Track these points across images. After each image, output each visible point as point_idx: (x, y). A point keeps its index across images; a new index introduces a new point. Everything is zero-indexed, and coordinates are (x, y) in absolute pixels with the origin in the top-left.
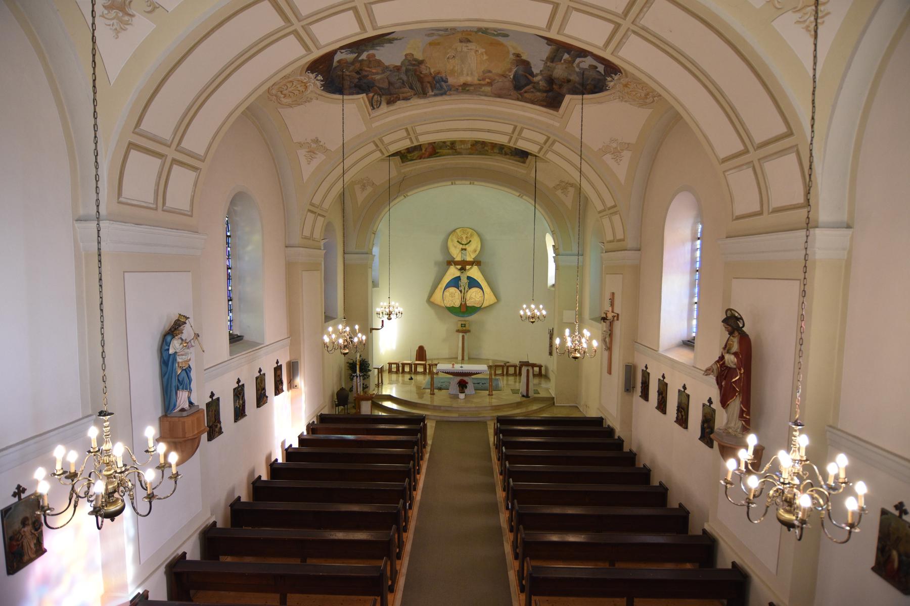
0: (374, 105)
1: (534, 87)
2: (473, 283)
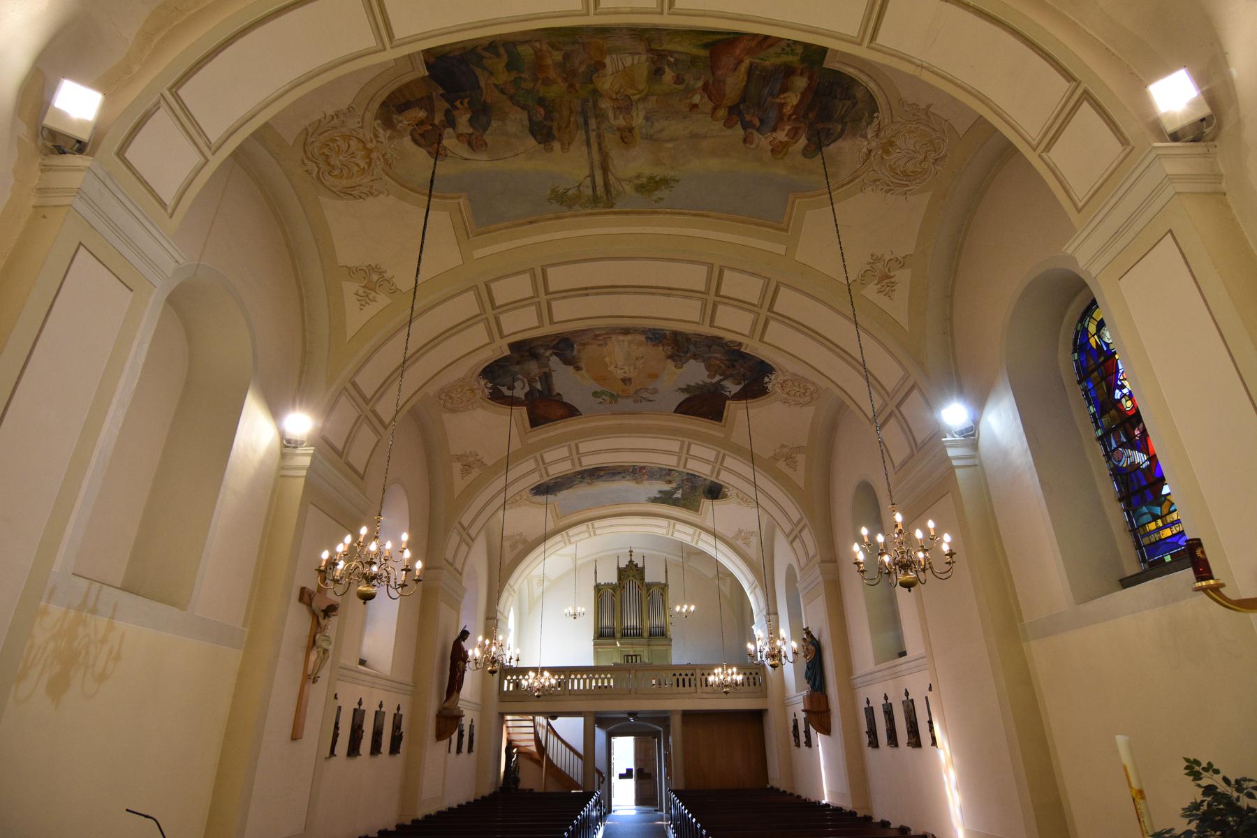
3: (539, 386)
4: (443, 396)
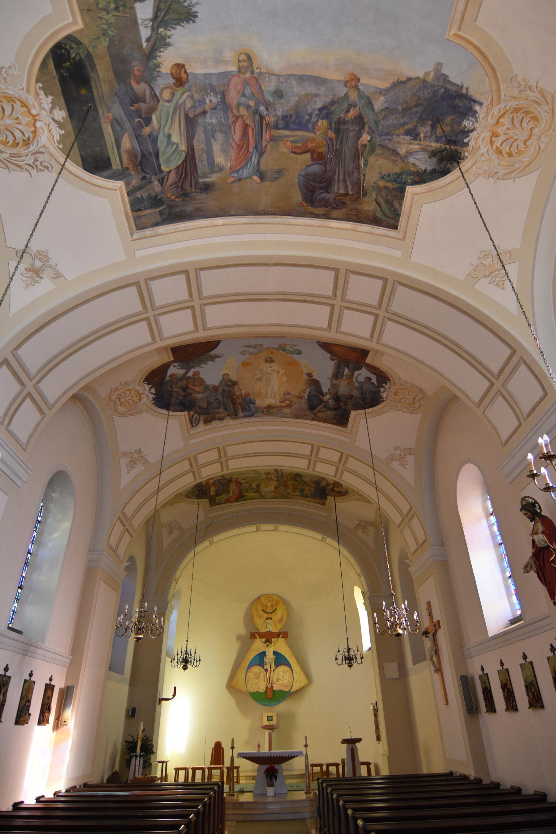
0: (193, 423)
1: (325, 406)
2: (280, 660)
3: (346, 371)
4: (417, 405)
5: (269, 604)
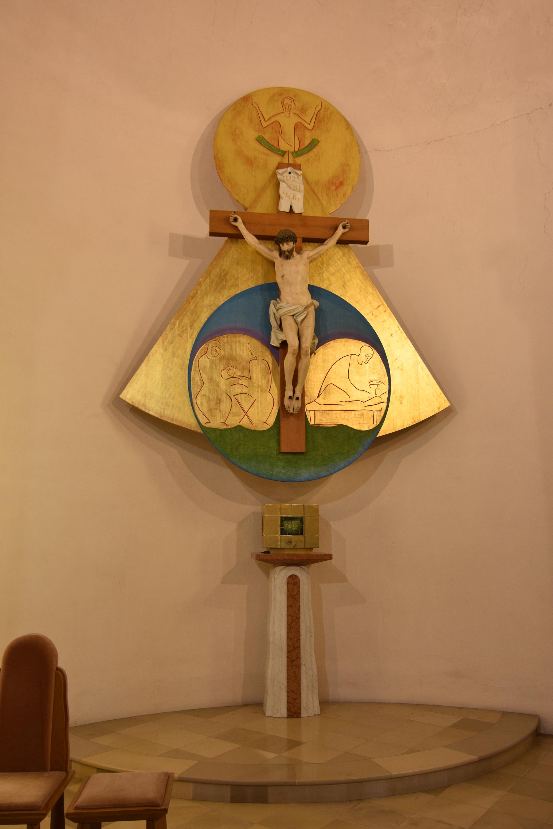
5: (288, 123)
